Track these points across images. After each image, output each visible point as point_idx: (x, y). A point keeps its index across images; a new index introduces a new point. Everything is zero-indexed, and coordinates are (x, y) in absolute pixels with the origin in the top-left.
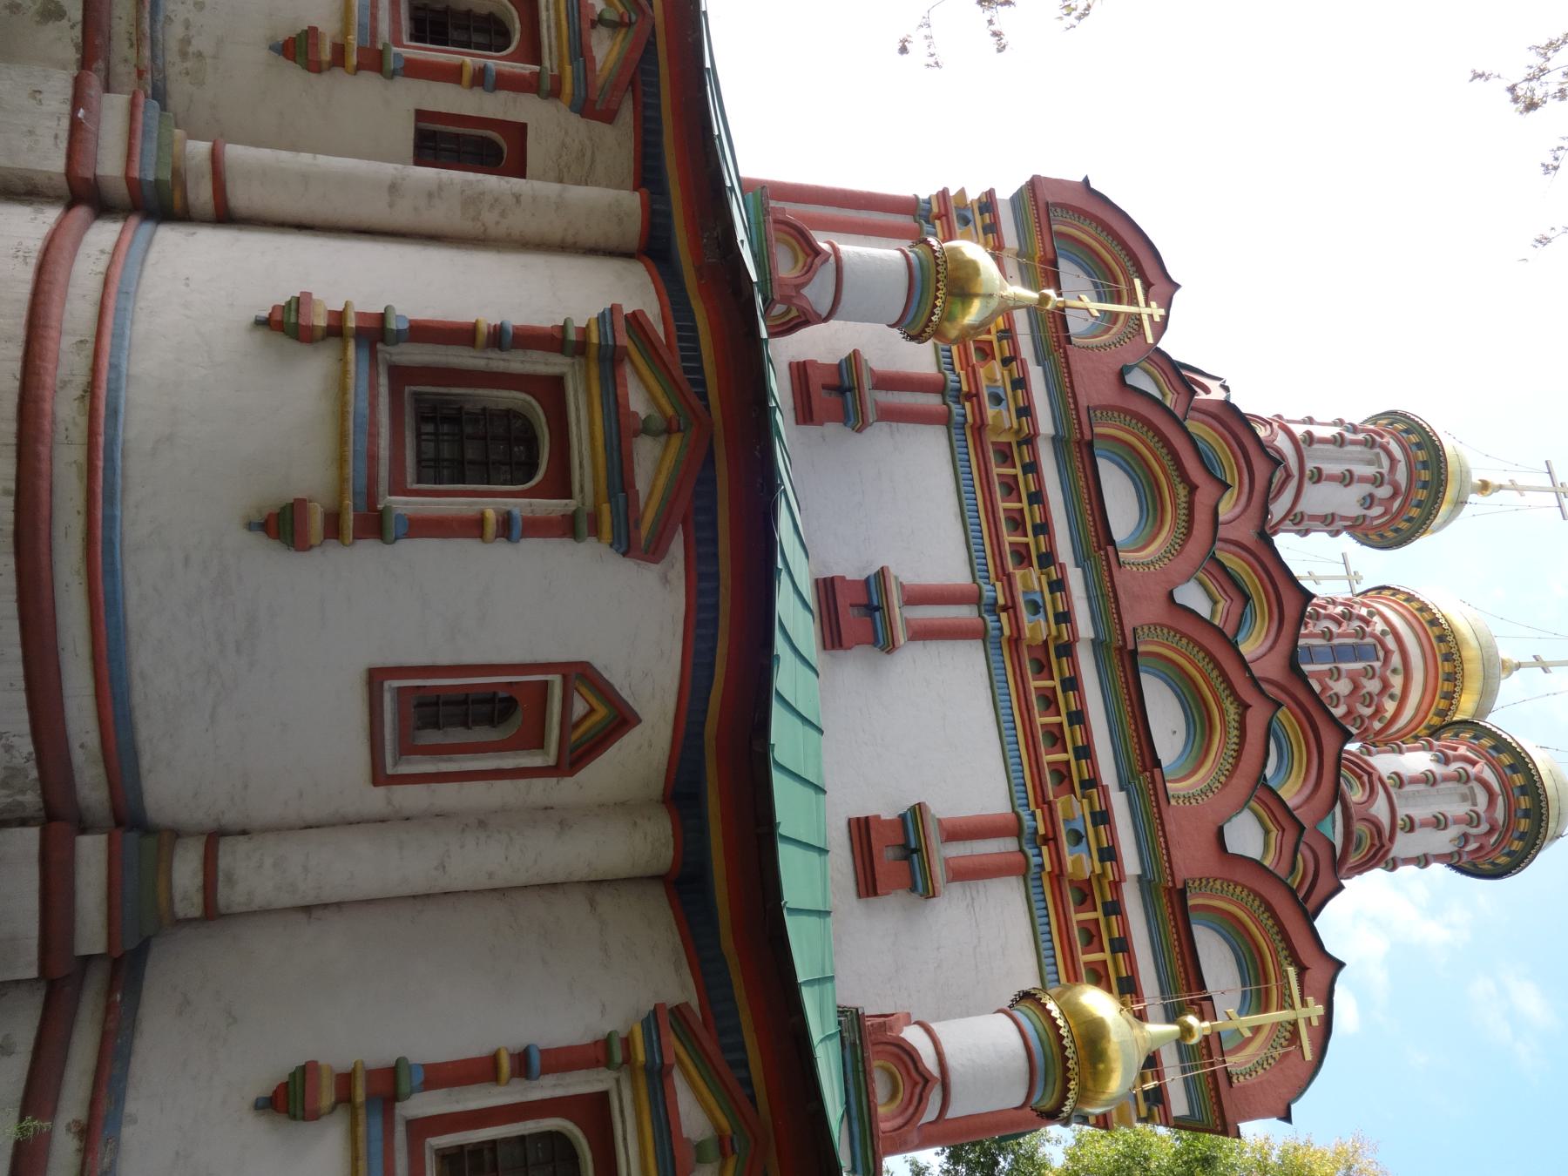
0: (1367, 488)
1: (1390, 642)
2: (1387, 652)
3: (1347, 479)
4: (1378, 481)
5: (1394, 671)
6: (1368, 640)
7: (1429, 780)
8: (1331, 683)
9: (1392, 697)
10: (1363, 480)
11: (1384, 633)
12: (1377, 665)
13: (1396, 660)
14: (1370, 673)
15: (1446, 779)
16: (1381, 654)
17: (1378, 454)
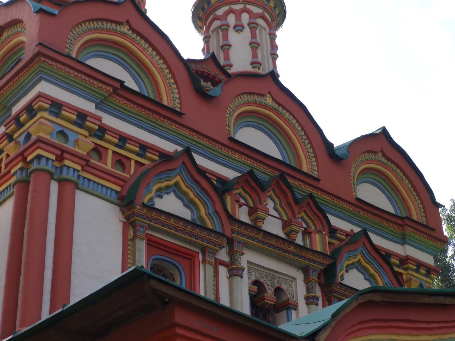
15: (253, 35)
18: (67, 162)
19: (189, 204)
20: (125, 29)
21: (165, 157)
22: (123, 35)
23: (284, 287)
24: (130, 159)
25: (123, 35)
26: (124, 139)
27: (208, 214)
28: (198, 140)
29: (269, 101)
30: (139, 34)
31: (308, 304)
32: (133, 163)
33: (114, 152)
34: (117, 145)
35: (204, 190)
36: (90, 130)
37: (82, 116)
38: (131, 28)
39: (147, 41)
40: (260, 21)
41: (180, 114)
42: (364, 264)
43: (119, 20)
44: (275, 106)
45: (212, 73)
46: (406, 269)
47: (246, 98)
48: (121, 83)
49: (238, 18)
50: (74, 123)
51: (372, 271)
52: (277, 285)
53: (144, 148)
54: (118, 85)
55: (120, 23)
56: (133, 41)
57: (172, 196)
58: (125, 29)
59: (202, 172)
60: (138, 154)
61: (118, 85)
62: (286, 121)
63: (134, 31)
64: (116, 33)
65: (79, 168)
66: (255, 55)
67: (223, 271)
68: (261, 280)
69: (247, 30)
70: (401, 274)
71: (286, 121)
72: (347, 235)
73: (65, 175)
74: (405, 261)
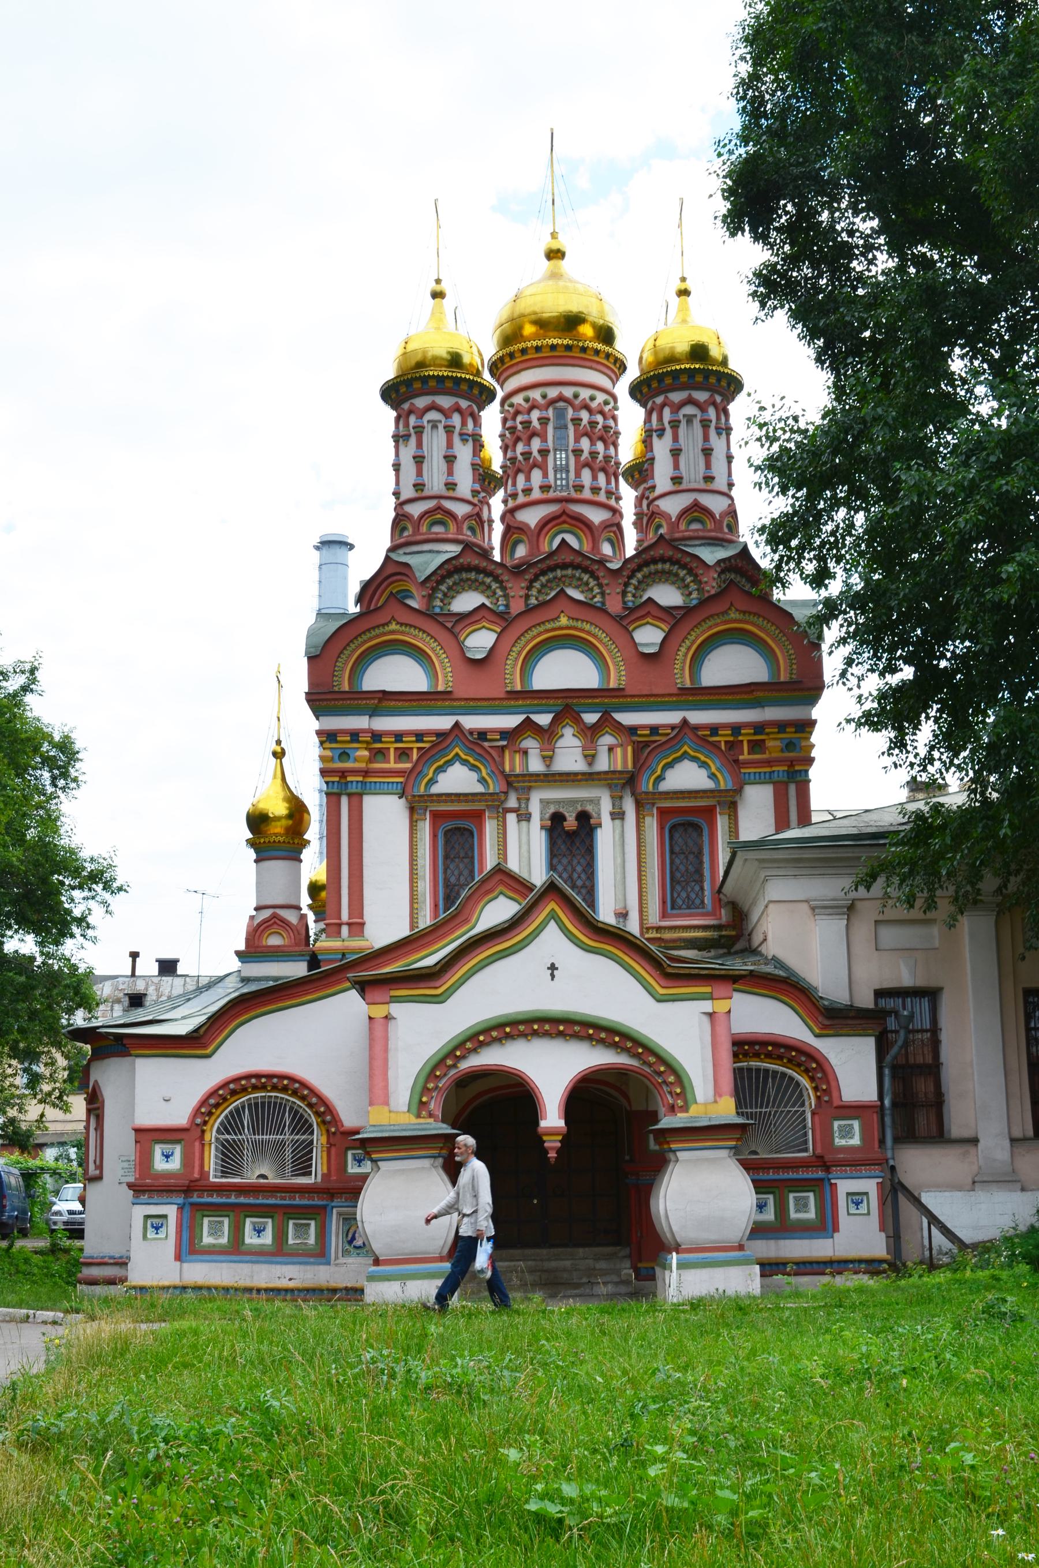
0: (456, 439)
1: (553, 393)
2: (561, 398)
3: (450, 460)
4: (449, 430)
5: (576, 396)
6: (550, 413)
7: (676, 453)
8: (583, 458)
9: (592, 398)
10: (450, 445)
11: (544, 397)
12: (570, 413)
13: (568, 392)
14: (577, 421)
15: (675, 438)
16: (561, 404)
17: (428, 422)
18: (349, 779)
19: (473, 768)
20: (393, 626)
21: (441, 735)
22: (393, 632)
23: (589, 808)
24: (412, 749)
25: (393, 632)
26: (399, 736)
27: (488, 774)
28: (475, 704)
29: (564, 621)
30: (406, 625)
31: (613, 819)
32: (415, 751)
33: (396, 749)
34: (396, 741)
35: (479, 754)
36: (367, 742)
37: (355, 735)
38: (398, 623)
39: (415, 628)
40: (689, 410)
41: (450, 692)
42: (692, 753)
43: (383, 621)
44: (572, 623)
45: (567, 560)
46: (768, 734)
47: (535, 631)
48: (384, 692)
49: (660, 419)
50: (352, 741)
51: (703, 758)
52: (580, 809)
53: (419, 736)
54: (381, 695)
55: (387, 624)
56: (402, 633)
57: (457, 765)
58: (393, 626)
59: (482, 734)
60: (417, 741)
61: (381, 695)
62: (589, 633)
63: (401, 624)
64: (384, 634)
65: (360, 779)
66: (676, 466)
67: (511, 818)
68: (561, 810)
69: (669, 432)
70: (763, 741)
71: (589, 633)
72: (673, 727)
73: (349, 791)
74: (759, 728)
